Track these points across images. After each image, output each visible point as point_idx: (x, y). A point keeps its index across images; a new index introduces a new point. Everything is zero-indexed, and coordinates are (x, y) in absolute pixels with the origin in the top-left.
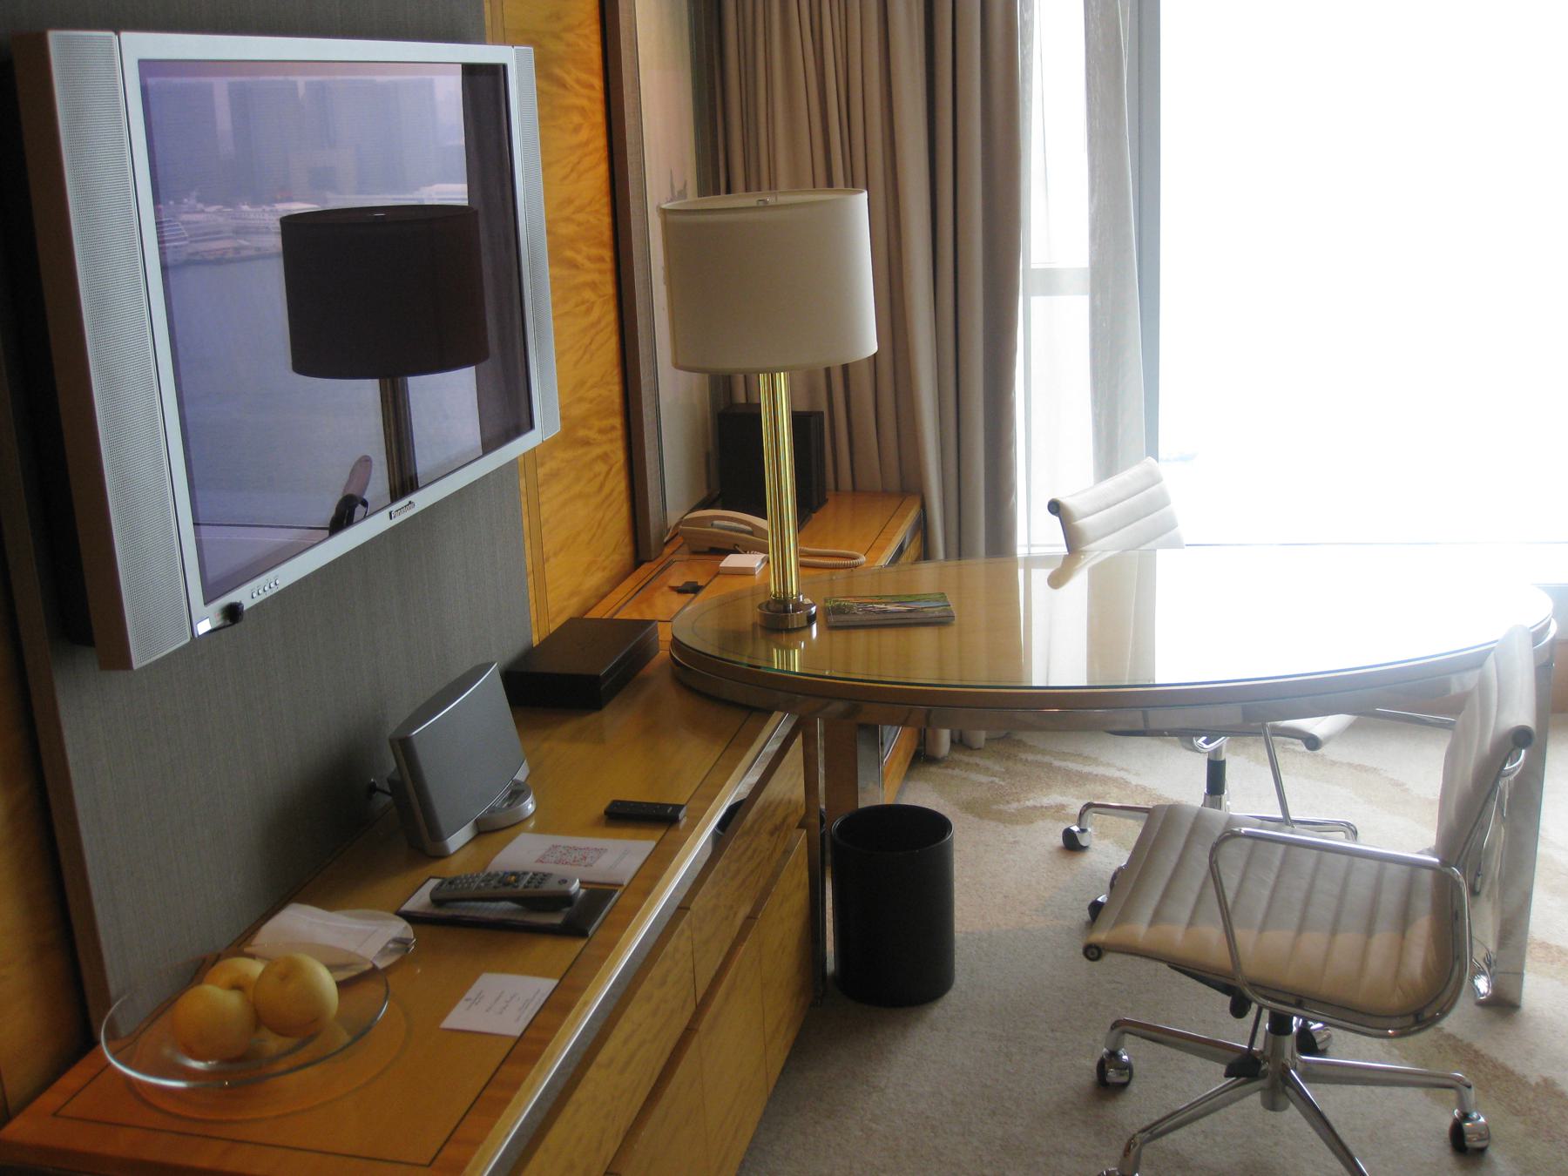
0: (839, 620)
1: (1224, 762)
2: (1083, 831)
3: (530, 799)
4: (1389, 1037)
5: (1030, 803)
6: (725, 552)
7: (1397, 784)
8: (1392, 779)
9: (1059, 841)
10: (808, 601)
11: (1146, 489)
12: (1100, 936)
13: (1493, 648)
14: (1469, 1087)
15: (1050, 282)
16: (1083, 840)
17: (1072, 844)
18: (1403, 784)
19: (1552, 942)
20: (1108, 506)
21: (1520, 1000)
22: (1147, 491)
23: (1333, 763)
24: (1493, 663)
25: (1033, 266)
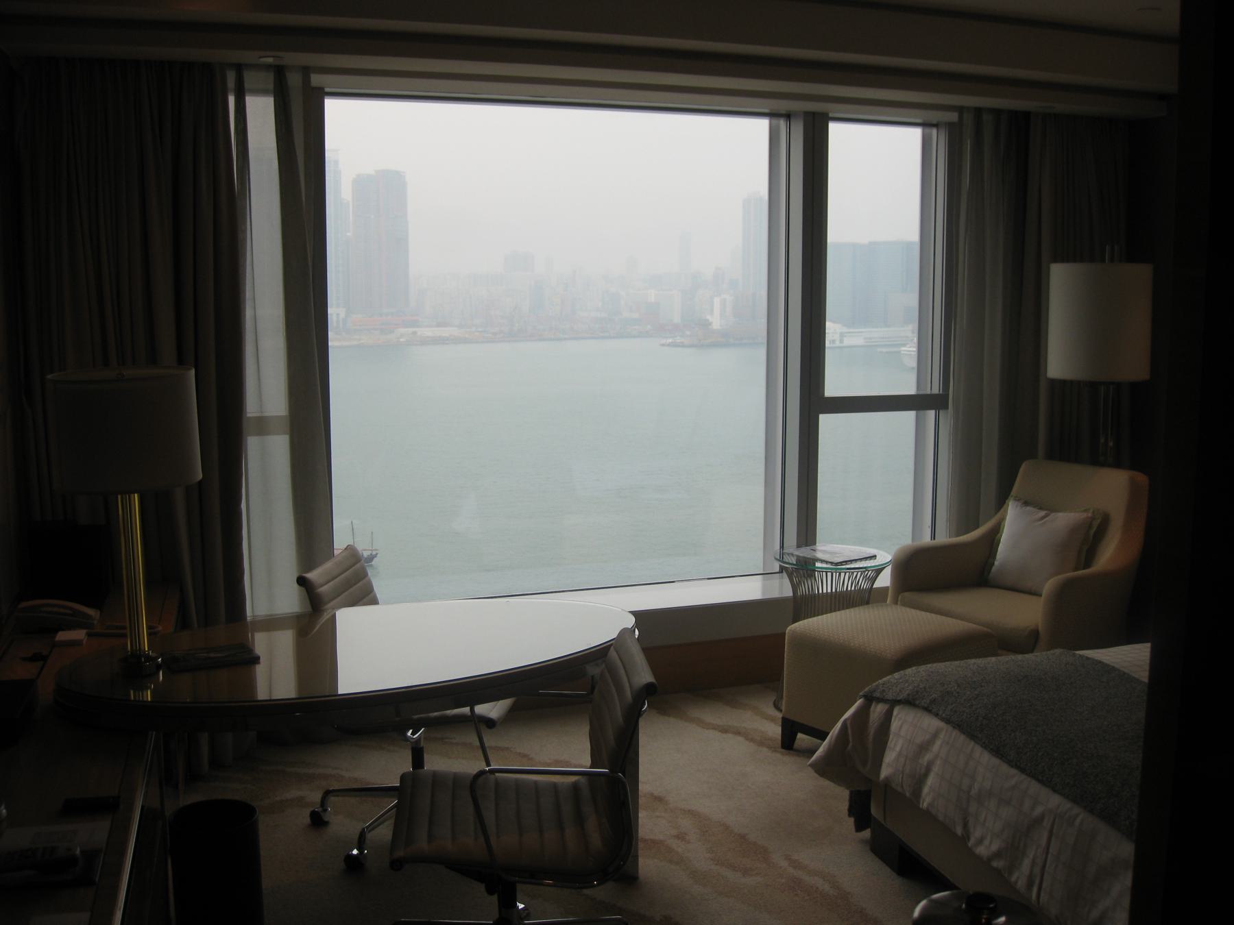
0: (174, 665)
2: (325, 810)
3: (3, 807)
4: (595, 886)
6: (56, 631)
7: (525, 756)
8: (520, 753)
9: (308, 820)
11: (354, 565)
12: (400, 853)
13: (612, 645)
15: (263, 426)
17: (318, 821)
19: (647, 837)
20: (333, 579)
21: (638, 872)
22: (354, 568)
25: (249, 415)
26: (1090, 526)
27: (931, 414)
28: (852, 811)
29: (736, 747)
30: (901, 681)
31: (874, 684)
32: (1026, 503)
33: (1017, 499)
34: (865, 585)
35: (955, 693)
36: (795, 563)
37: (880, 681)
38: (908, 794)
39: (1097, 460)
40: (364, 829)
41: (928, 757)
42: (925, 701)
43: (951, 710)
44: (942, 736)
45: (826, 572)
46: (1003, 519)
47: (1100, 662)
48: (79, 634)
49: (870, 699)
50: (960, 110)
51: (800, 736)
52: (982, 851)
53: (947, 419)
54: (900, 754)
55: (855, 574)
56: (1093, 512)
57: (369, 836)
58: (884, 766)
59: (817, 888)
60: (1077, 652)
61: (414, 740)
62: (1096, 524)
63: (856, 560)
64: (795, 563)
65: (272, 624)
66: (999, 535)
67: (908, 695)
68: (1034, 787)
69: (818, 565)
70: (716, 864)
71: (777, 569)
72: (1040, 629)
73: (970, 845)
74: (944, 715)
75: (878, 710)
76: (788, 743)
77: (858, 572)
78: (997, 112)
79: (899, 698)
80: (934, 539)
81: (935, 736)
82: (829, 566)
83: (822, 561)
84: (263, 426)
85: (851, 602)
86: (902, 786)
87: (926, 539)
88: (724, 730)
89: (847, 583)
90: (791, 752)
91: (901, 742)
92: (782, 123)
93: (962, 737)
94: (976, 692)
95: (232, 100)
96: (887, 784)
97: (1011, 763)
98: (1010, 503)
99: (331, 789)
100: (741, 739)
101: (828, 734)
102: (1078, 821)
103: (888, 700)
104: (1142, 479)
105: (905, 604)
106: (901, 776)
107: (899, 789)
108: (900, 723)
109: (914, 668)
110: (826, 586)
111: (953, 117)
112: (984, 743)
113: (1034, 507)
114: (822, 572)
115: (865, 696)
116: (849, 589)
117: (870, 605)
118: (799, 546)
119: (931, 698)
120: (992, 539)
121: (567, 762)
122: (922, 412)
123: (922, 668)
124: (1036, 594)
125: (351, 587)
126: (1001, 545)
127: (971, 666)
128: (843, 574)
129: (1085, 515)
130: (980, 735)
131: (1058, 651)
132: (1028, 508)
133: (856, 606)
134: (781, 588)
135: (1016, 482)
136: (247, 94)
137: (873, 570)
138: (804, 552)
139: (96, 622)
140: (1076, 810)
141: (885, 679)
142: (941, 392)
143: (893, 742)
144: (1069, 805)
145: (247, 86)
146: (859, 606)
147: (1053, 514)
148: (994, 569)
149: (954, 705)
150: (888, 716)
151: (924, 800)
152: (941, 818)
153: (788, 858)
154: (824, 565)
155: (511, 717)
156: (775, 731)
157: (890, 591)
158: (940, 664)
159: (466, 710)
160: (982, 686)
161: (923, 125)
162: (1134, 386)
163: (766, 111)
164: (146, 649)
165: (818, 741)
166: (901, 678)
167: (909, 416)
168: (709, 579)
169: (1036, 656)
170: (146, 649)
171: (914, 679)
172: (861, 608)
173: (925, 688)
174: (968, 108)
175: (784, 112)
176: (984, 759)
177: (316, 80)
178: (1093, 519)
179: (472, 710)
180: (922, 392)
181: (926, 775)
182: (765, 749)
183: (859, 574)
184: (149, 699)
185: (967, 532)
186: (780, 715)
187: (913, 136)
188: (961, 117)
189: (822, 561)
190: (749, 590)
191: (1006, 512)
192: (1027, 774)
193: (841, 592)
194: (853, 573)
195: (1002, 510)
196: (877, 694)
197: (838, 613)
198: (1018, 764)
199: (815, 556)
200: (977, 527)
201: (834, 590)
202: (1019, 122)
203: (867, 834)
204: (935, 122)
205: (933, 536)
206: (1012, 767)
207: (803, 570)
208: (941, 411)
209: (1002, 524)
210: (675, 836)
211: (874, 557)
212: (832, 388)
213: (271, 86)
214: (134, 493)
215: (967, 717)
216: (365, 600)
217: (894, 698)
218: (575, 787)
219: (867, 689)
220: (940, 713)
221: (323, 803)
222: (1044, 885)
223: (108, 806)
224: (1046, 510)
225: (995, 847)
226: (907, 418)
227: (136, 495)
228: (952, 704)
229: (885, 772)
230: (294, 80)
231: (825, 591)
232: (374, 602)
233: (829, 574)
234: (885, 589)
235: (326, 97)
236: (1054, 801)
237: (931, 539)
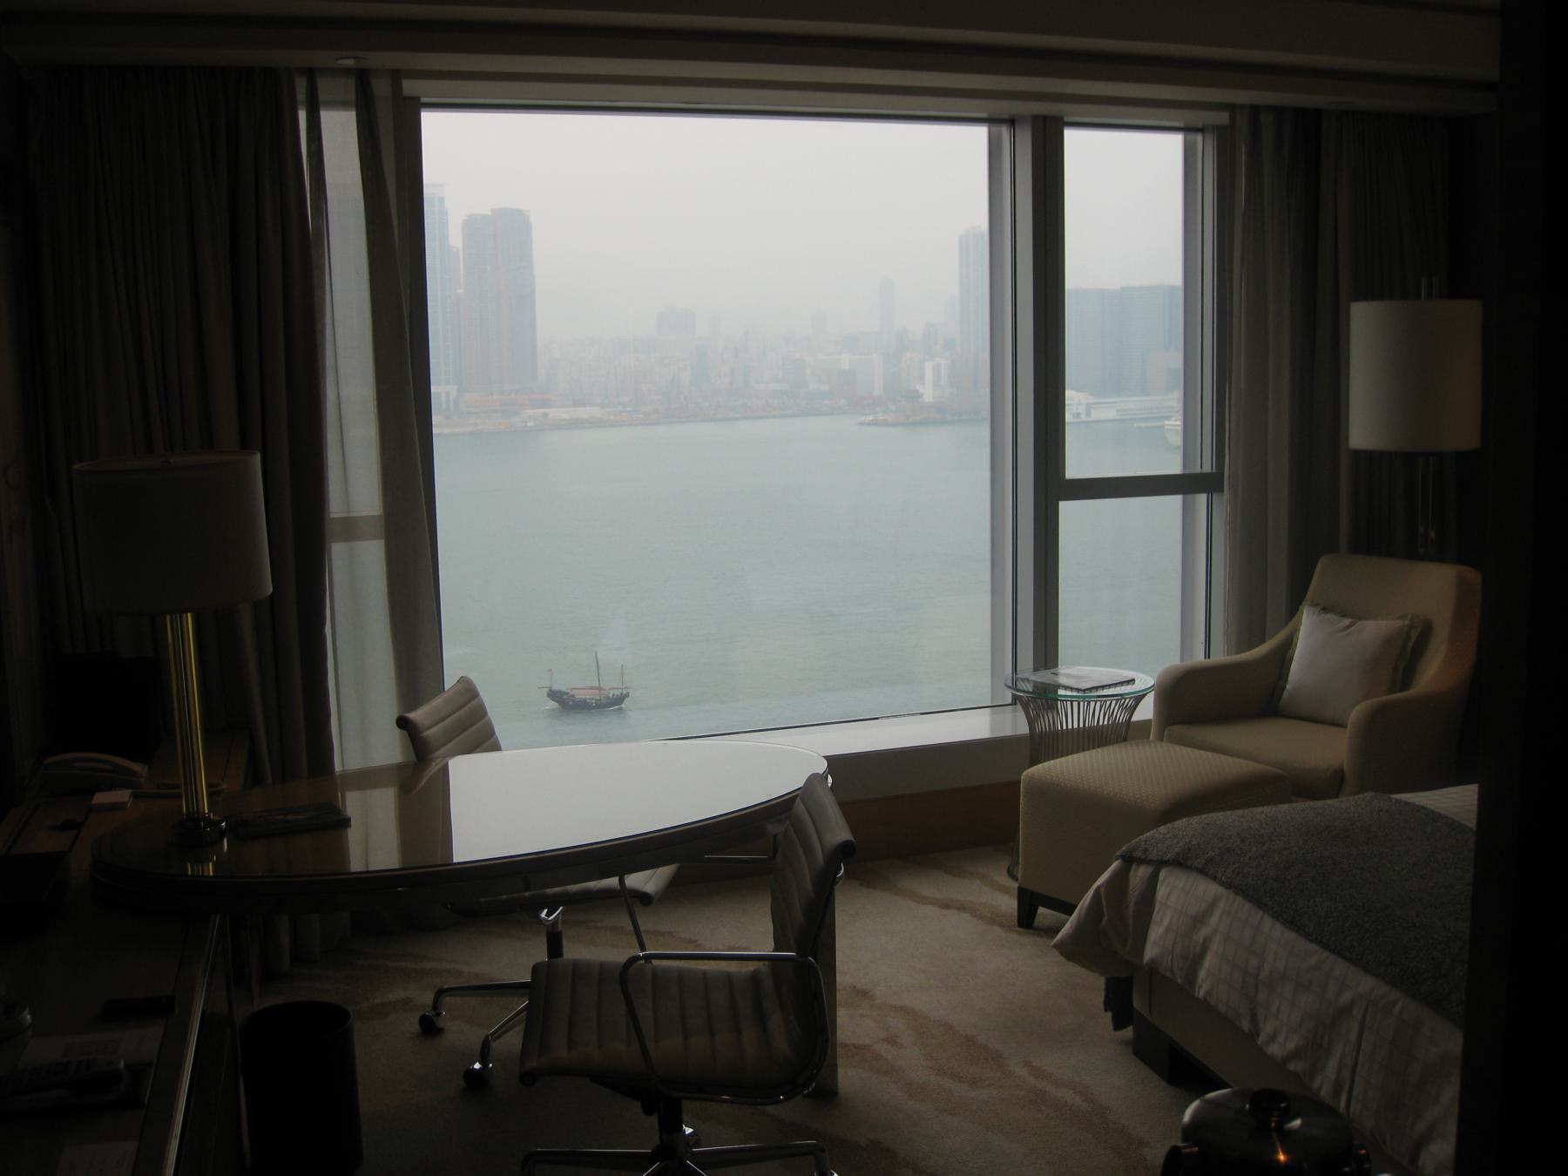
1: (561, 932)
2: (439, 1014)
3: (27, 1011)
5: (379, 1001)
6: (93, 792)
9: (416, 1028)
10: (216, 818)
11: (470, 701)
13: (797, 796)
14: (824, 1151)
15: (351, 529)
16: (440, 1024)
17: (429, 1028)
18: (696, 941)
19: (848, 1042)
21: (836, 1085)
22: (469, 705)
24: (802, 805)
25: (334, 516)
27: (1202, 499)
28: (1108, 1005)
29: (959, 926)
30: (1168, 836)
31: (1133, 842)
32: (1325, 610)
33: (1313, 604)
34: (1121, 717)
36: (1031, 690)
38: (1179, 981)
39: (1414, 553)
40: (487, 1037)
41: (1204, 932)
42: (1199, 860)
44: (1221, 905)
45: (1072, 702)
46: (1296, 631)
47: (1424, 808)
48: (122, 796)
49: (1129, 861)
50: (1232, 108)
51: (1041, 910)
52: (1275, 1050)
53: (1222, 504)
54: (1168, 929)
55: (1108, 703)
56: (1411, 620)
57: (496, 1046)
58: (1148, 946)
59: (1066, 1102)
61: (548, 923)
62: (1414, 634)
63: (1109, 686)
64: (1031, 690)
65: (366, 779)
66: (1291, 651)
68: (1340, 967)
70: (937, 1074)
71: (1009, 700)
72: (1345, 768)
73: (1259, 1043)
74: (1223, 878)
75: (1140, 873)
76: (1026, 920)
78: (1278, 111)
79: (1167, 858)
80: (1209, 657)
81: (1213, 905)
82: (1075, 694)
83: (1066, 688)
84: (351, 529)
86: (1172, 971)
87: (1199, 658)
88: (945, 905)
89: (1098, 716)
90: (1031, 931)
91: (1169, 914)
92: (1005, 131)
93: (1248, 906)
94: (1265, 848)
95: (302, 116)
96: (1153, 969)
97: (1309, 937)
98: (1305, 611)
99: (445, 987)
100: (966, 916)
101: (1077, 906)
102: (1397, 1008)
103: (1151, 861)
104: (1474, 576)
105: (1173, 741)
107: (1168, 974)
109: (1184, 820)
110: (1071, 719)
111: (1223, 118)
113: (1335, 614)
115: (1122, 857)
116: (1101, 723)
117: (1127, 743)
118: (1036, 669)
120: (1282, 656)
123: (1196, 819)
124: (1338, 724)
125: (466, 729)
127: (1258, 816)
128: (1092, 704)
129: (1399, 623)
130: (1270, 903)
131: (1368, 795)
132: (1329, 616)
133: (1110, 744)
134: (1015, 724)
136: (321, 108)
137: (1131, 698)
138: (1043, 677)
139: (142, 780)
141: (1148, 834)
142: (1214, 470)
145: (322, 97)
146: (1114, 743)
147: (1360, 622)
148: (1285, 694)
150: (1153, 881)
151: (1200, 987)
152: (1222, 1009)
153: (1027, 1064)
154: (1069, 693)
155: (676, 891)
156: (1009, 905)
159: (613, 882)
161: (1185, 129)
163: (984, 115)
164: (206, 811)
165: (1062, 916)
166: (1168, 833)
167: (1174, 502)
169: (1341, 802)
170: (206, 811)
173: (1199, 844)
175: (1006, 116)
176: (1275, 931)
177: (410, 87)
178: (1411, 627)
179: (622, 882)
180: (1188, 472)
182: (997, 930)
183: (1114, 702)
184: (211, 874)
185: (1250, 648)
186: (1015, 885)
188: (1232, 119)
189: (1066, 688)
190: (974, 727)
191: (1300, 622)
192: (1330, 951)
193: (1090, 728)
194: (1106, 701)
195: (1295, 620)
196: (1138, 854)
197: (1087, 753)
198: (1319, 937)
199: (1056, 682)
200: (1263, 641)
201: (1081, 725)
202: (1307, 123)
203: (1128, 1032)
204: (1200, 126)
205: (1208, 654)
206: (1311, 941)
207: (1041, 699)
210: (883, 1040)
211: (1132, 681)
212: (1077, 466)
213: (352, 97)
216: (484, 746)
217: (1160, 858)
218: (755, 978)
219: (1124, 848)
220: (1219, 875)
221: (436, 1006)
222: (1355, 1093)
223: (161, 1009)
224: (1350, 617)
225: (1291, 1045)
227: (189, 614)
228: (1234, 864)
229: (1149, 953)
230: (381, 88)
231: (1070, 727)
232: (496, 747)
233: (1075, 704)
234: (1147, 723)
235: (422, 109)
236: (1366, 984)
237: (1205, 658)
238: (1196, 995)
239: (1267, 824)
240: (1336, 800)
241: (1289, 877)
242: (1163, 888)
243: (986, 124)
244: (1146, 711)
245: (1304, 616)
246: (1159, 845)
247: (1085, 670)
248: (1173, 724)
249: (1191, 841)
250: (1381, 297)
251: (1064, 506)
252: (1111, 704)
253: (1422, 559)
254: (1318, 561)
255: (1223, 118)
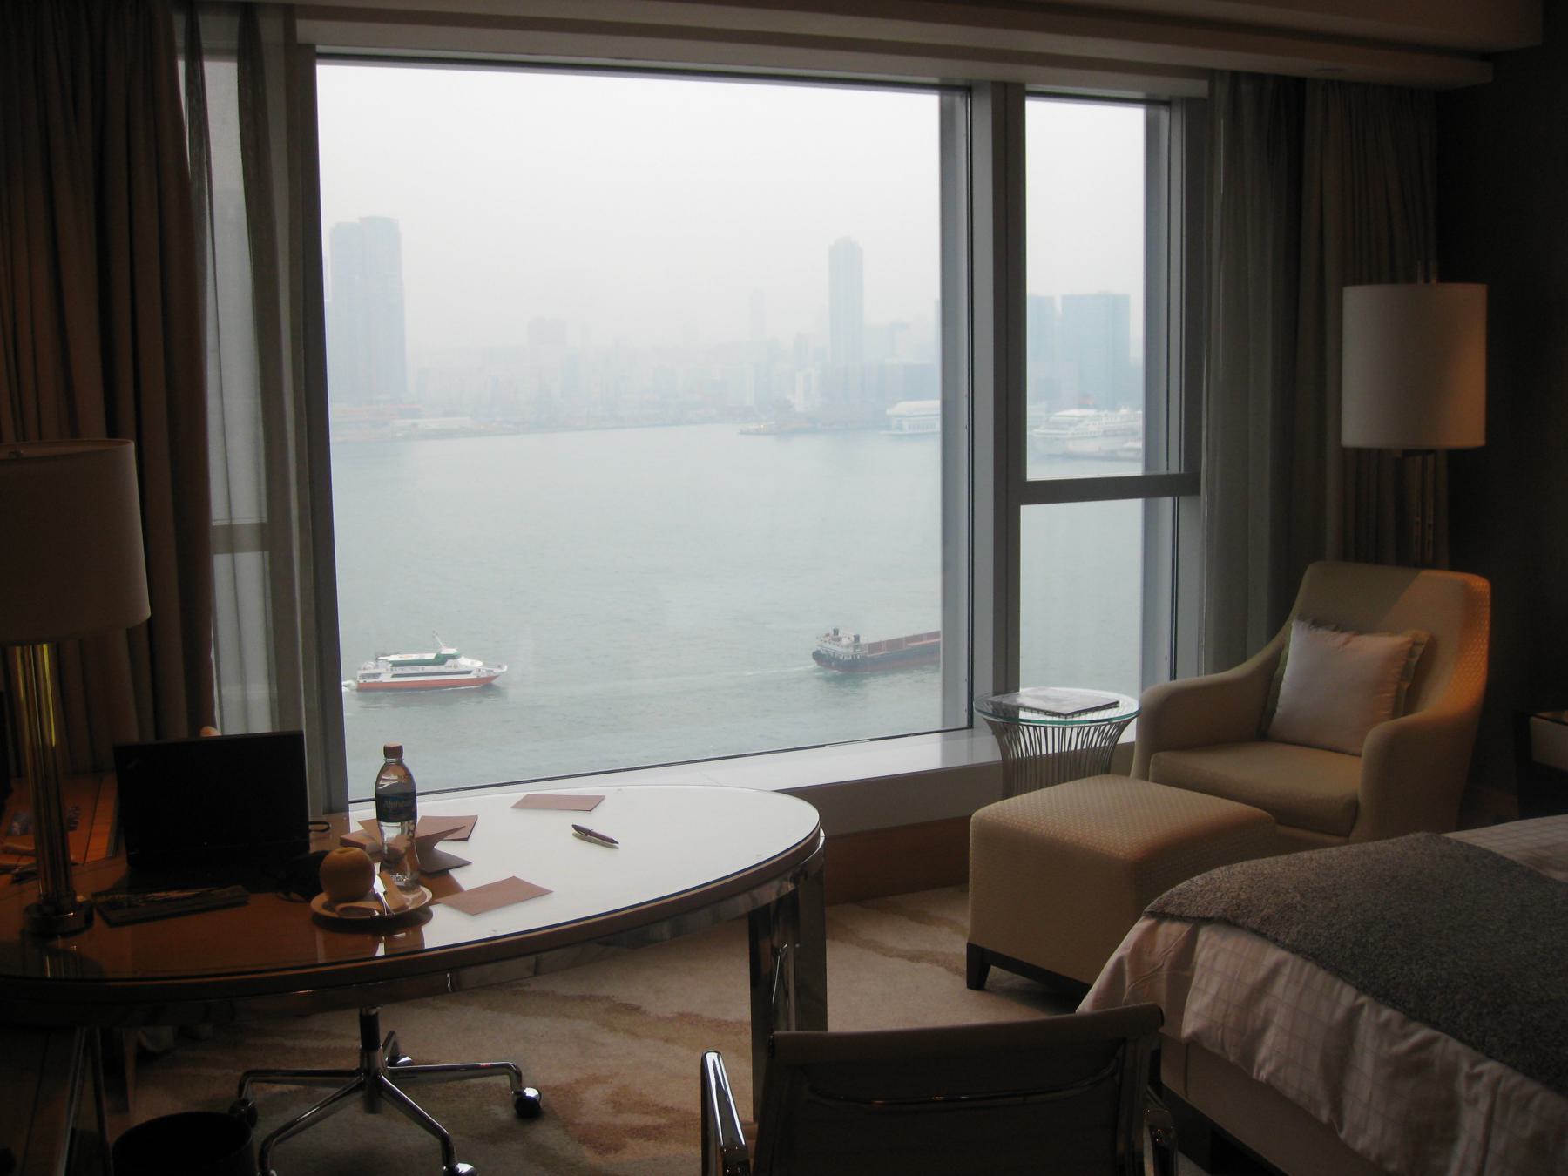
23: (566, 998)
26: (1411, 653)
27: (1166, 503)
30: (1207, 888)
31: (1164, 895)
33: (1301, 618)
35: (1299, 906)
36: (991, 711)
37: (1173, 889)
38: (1232, 1059)
39: (1411, 558)
41: (1266, 1003)
43: (1298, 932)
44: (1286, 970)
45: (1045, 728)
46: (1282, 648)
47: (1491, 853)
50: (1209, 74)
54: (1216, 998)
55: (1086, 729)
60: (1451, 835)
62: (1419, 650)
64: (991, 711)
66: (1278, 670)
67: (1224, 910)
69: (1023, 715)
71: (965, 724)
72: (1360, 800)
73: (1342, 1136)
77: (1090, 727)
78: (1257, 78)
79: (1211, 915)
80: (1175, 679)
81: (1275, 971)
83: (1026, 708)
85: (1082, 768)
86: (1223, 1048)
88: (915, 957)
92: (960, 102)
93: (1321, 974)
95: (181, 66)
96: (1195, 1042)
98: (1293, 624)
103: (1189, 917)
106: (1220, 1031)
107: (1217, 1051)
108: (1213, 951)
109: (1223, 868)
110: (1025, 745)
111: (1199, 88)
112: (1361, 983)
114: (1040, 727)
116: (1079, 747)
119: (1262, 914)
120: (1271, 672)
121: (697, 1016)
122: (1153, 500)
123: (1237, 868)
126: (1283, 683)
128: (1069, 730)
130: (1352, 972)
131: (1421, 835)
132: (1321, 632)
133: (1089, 776)
134: (983, 750)
135: (1299, 596)
136: (204, 57)
138: (1006, 700)
140: (1531, 1086)
141: (1180, 886)
143: (1204, 981)
144: (1516, 1078)
145: (206, 43)
146: (1094, 775)
148: (1276, 718)
149: (1300, 926)
151: (1261, 1067)
152: (1291, 1093)
157: (1136, 750)
158: (1261, 861)
160: (1337, 896)
162: (1457, 458)
163: (935, 80)
166: (1207, 884)
168: (872, 740)
171: (1228, 885)
172: (1097, 779)
173: (1249, 899)
174: (1222, 72)
177: (306, 29)
181: (1263, 1030)
183: (1093, 729)
185: (1229, 667)
187: (1131, 120)
189: (1026, 708)
190: (923, 756)
193: (1060, 753)
195: (1281, 634)
200: (1243, 659)
201: (1056, 751)
204: (1165, 98)
205: (1174, 674)
207: (1007, 723)
208: (1181, 498)
209: (1283, 654)
211: (1115, 704)
212: (1036, 471)
213: (234, 44)
214: (42, 642)
215: (1326, 943)
217: (1201, 916)
219: (1153, 903)
220: (1281, 938)
226: (1131, 510)
227: (45, 646)
228: (1298, 924)
229: (1189, 1026)
230: (271, 30)
234: (1130, 746)
235: (318, 61)
237: (1171, 679)
238: (1254, 1076)
239: (1323, 874)
240: (1387, 841)
241: (1371, 940)
242: (1206, 950)
243: (937, 92)
244: (1129, 735)
245: (1293, 632)
246: (1198, 899)
247: (1053, 691)
248: (1164, 750)
249: (1239, 894)
250: (1370, 282)
251: (1026, 510)
252: (1104, 728)
253: (1422, 564)
254: (1306, 568)
255: (1199, 88)
